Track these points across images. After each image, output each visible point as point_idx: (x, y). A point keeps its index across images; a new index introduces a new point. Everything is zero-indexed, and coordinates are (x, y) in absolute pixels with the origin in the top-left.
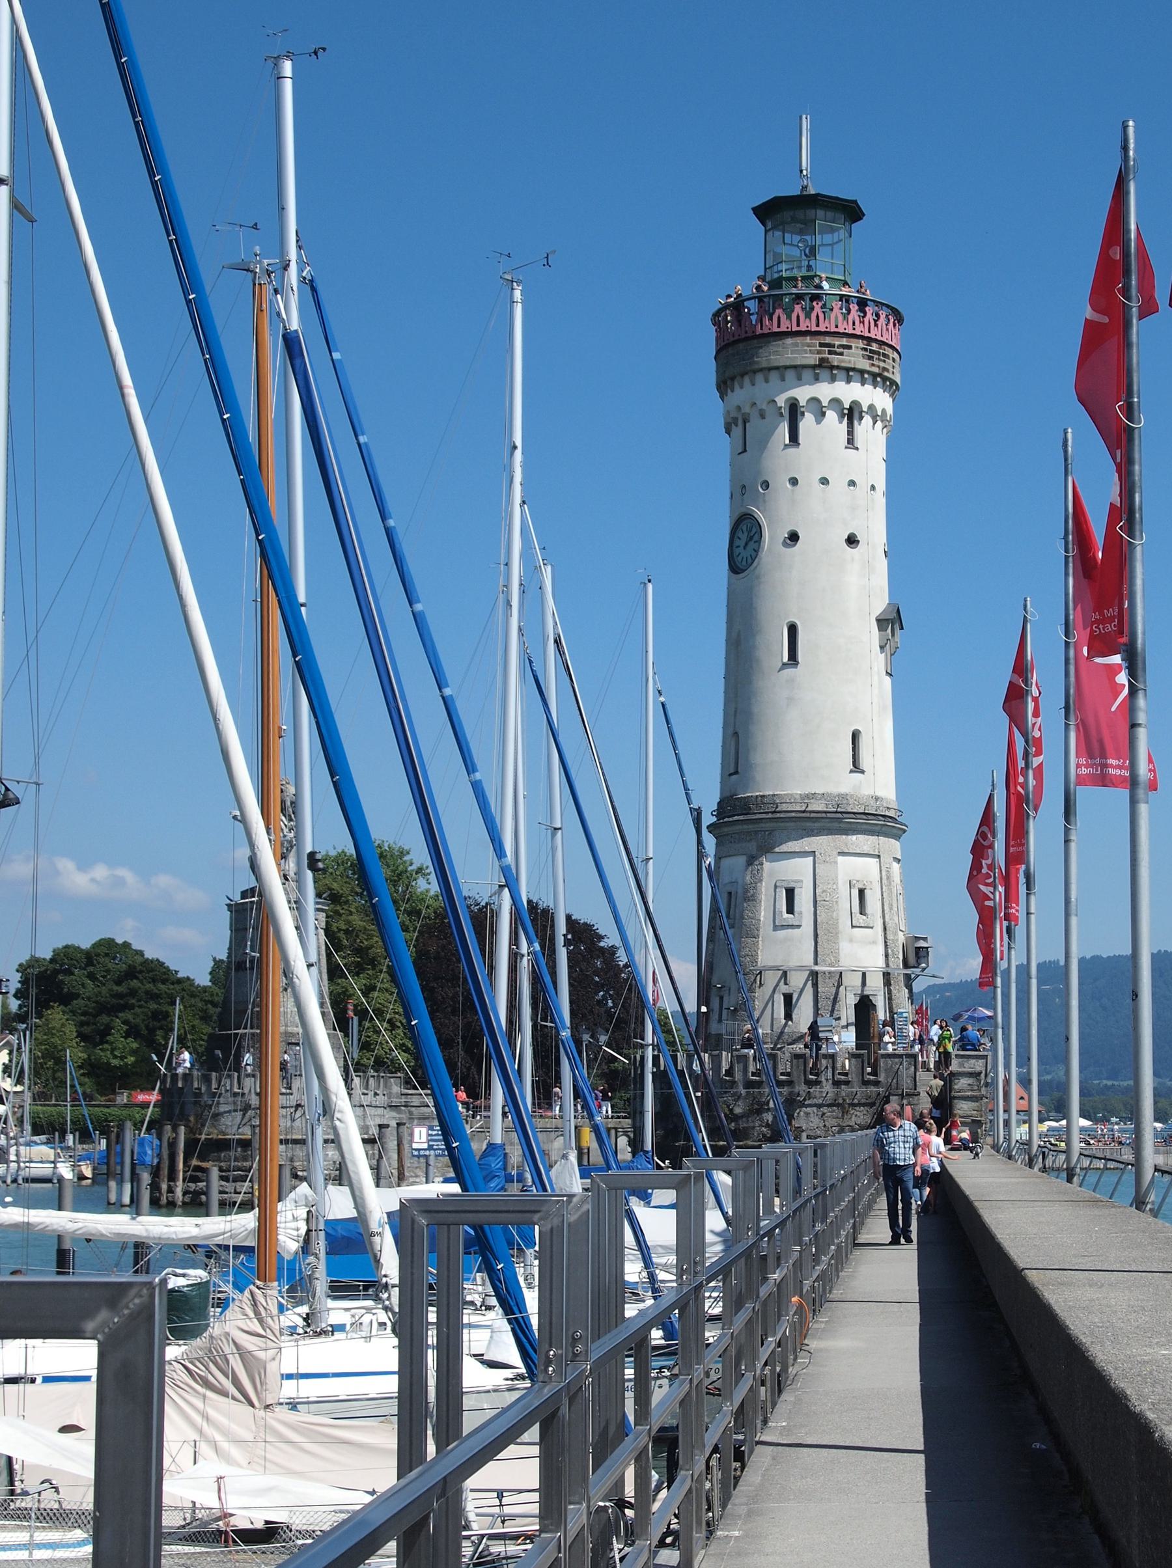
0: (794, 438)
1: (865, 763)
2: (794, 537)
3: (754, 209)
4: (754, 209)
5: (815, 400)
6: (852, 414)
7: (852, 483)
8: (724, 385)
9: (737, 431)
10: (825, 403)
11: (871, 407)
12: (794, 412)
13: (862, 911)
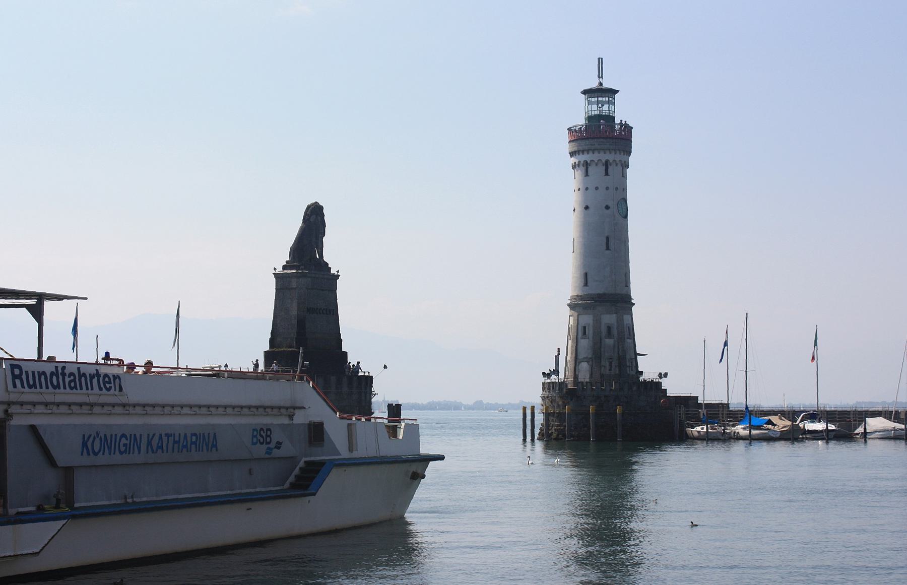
0: (607, 174)
2: (607, 207)
9: (583, 169)
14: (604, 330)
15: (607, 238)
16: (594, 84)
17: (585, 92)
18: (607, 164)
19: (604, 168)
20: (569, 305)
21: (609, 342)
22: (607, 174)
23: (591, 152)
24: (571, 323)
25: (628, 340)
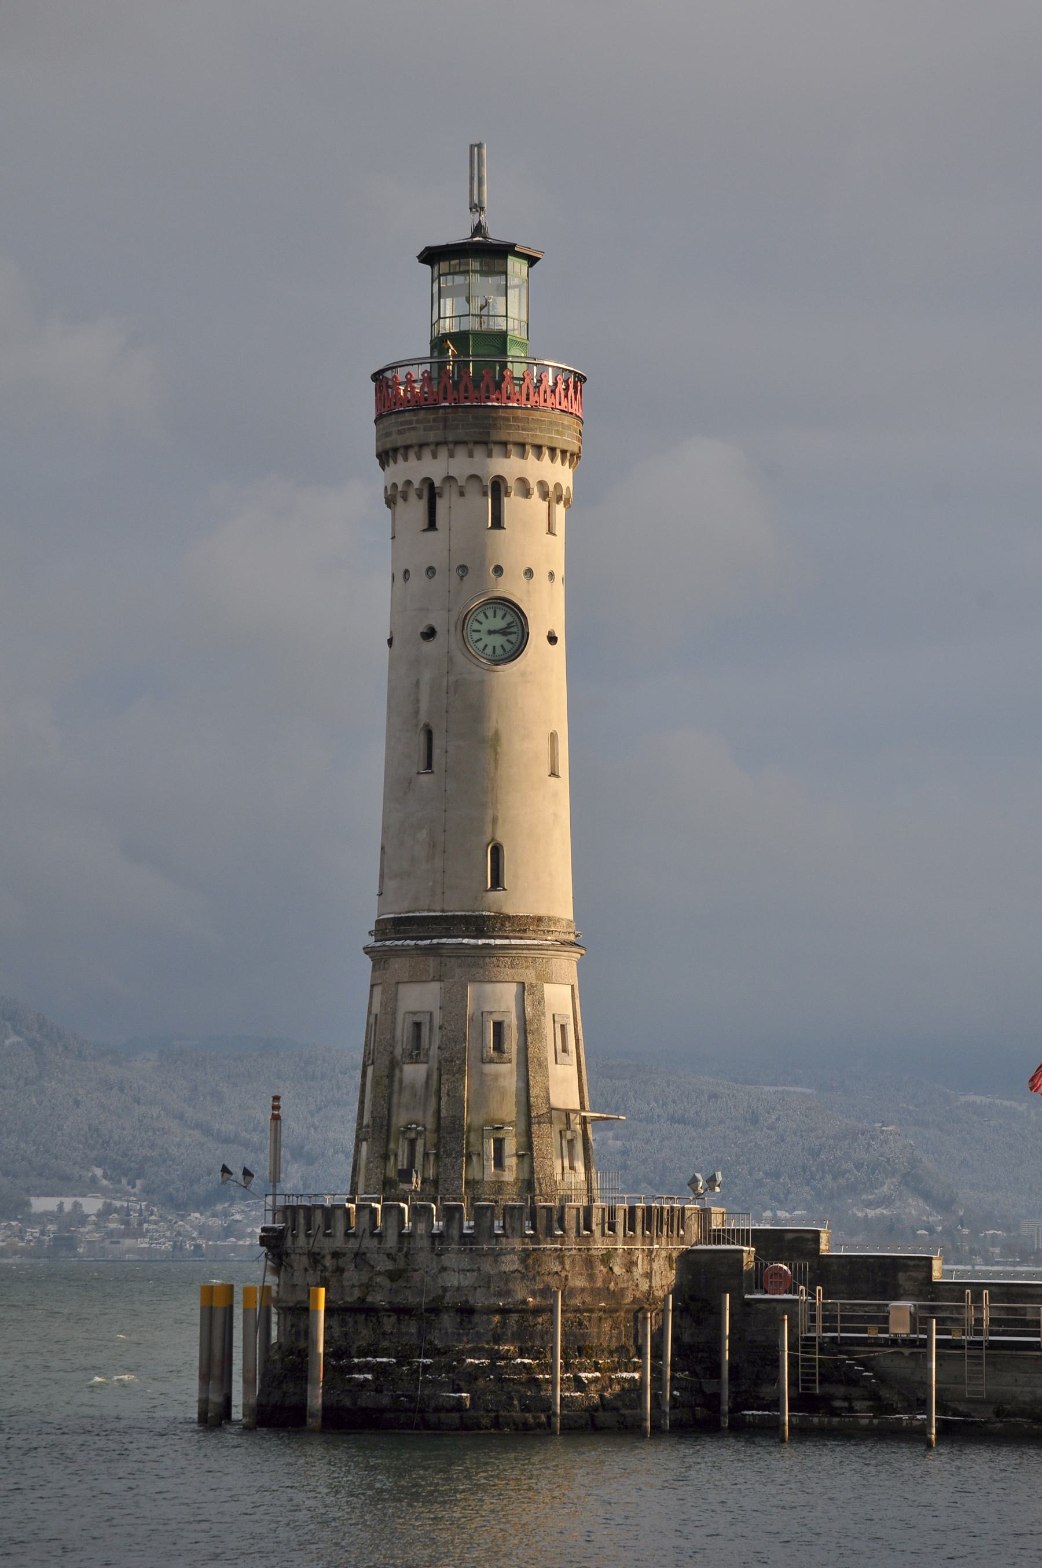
0: (432, 525)
1: (507, 880)
2: (430, 634)
3: (418, 257)
4: (418, 257)
5: (449, 479)
6: (498, 488)
7: (498, 570)
8: (385, 457)
10: (461, 482)
11: (523, 481)
12: (431, 493)
13: (499, 1046)
14: (403, 1032)
15: (429, 734)
16: (459, 233)
17: (431, 256)
18: (431, 493)
19: (422, 506)
20: (368, 951)
21: (414, 1073)
22: (432, 525)
23: (443, 452)
24: (376, 1008)
25: (490, 1068)
